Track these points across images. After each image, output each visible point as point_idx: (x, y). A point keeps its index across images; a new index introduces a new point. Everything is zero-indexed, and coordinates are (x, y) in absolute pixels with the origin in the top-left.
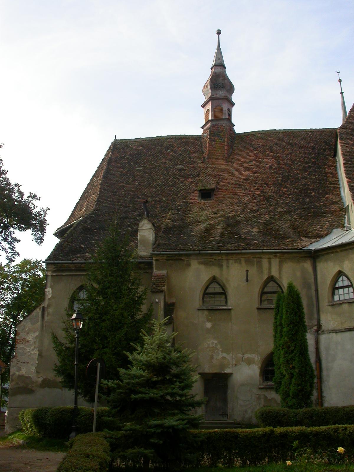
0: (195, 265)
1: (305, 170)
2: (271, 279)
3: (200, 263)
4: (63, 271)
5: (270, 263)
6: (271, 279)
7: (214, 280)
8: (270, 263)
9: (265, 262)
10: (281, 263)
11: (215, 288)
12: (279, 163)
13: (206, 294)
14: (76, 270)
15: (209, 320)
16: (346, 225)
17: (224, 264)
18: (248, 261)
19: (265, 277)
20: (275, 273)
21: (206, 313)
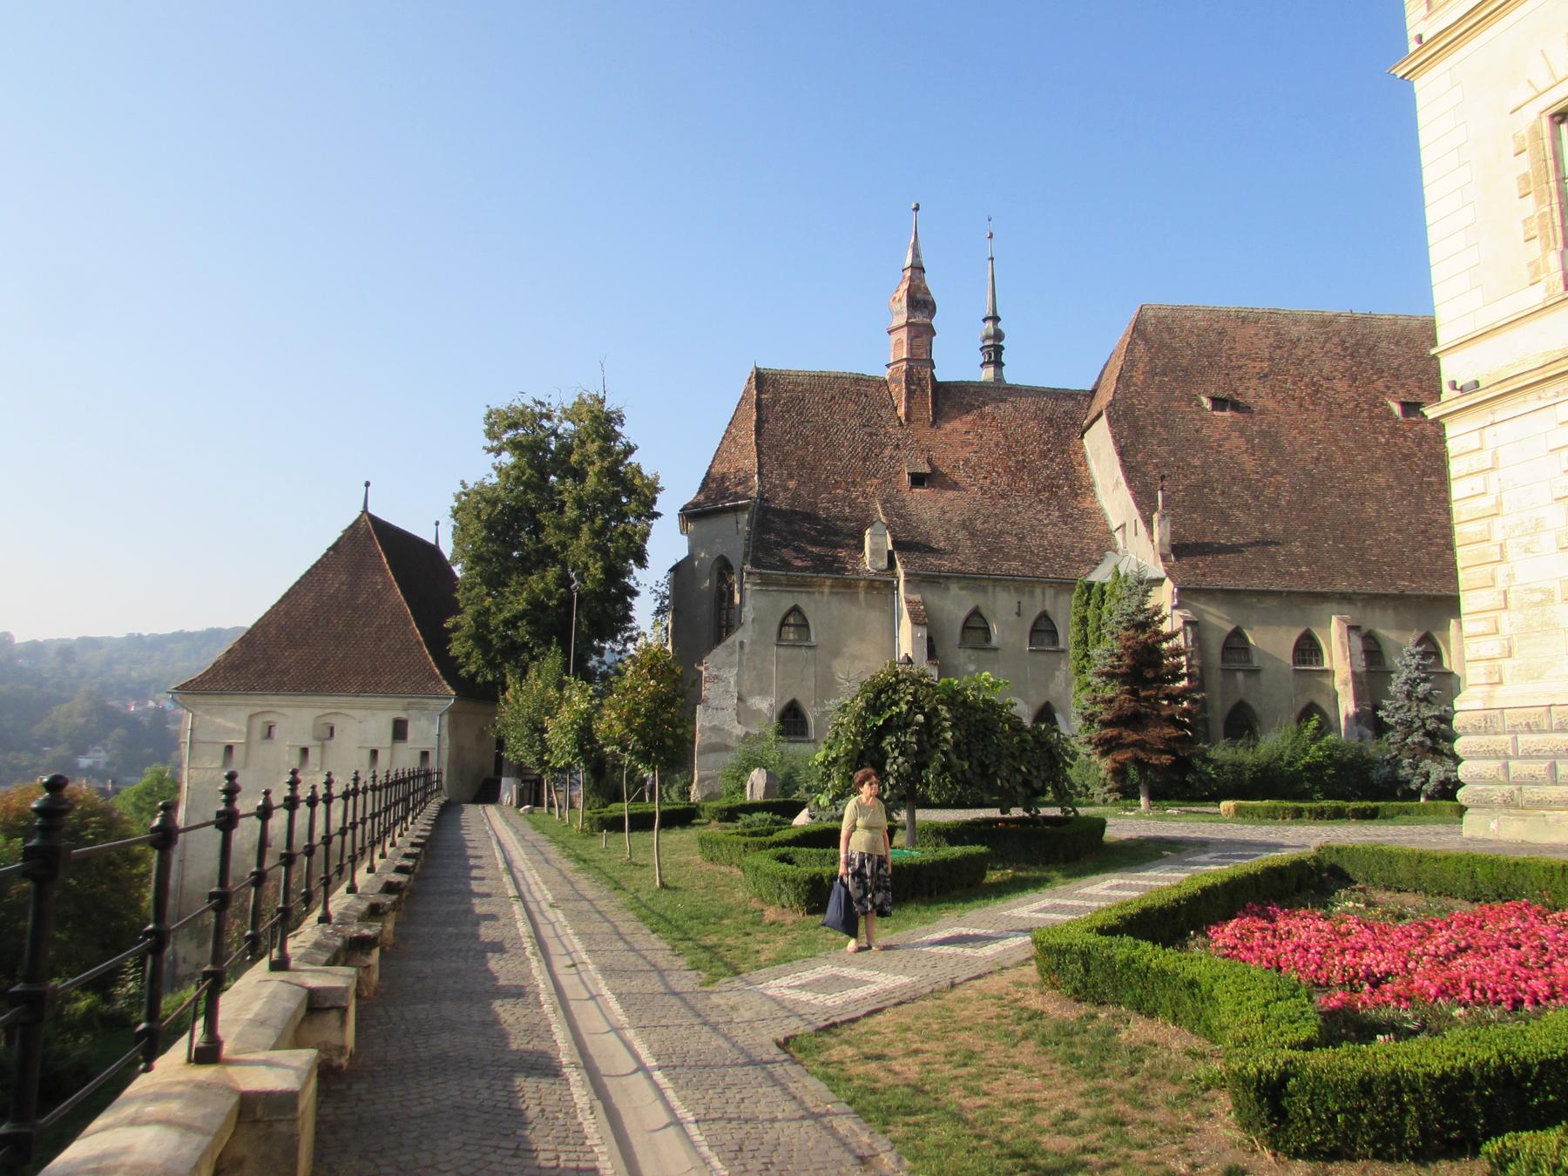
0: (954, 588)
1: (1043, 455)
2: (1044, 616)
3: (962, 588)
4: (767, 585)
5: (1044, 593)
6: (1044, 616)
7: (976, 613)
8: (1044, 593)
9: (1038, 591)
10: (1056, 595)
11: (976, 623)
12: (1006, 436)
13: (966, 627)
14: (788, 585)
15: (970, 661)
16: (1120, 545)
17: (990, 589)
18: (1018, 590)
19: (1038, 611)
20: (1048, 607)
21: (969, 652)
